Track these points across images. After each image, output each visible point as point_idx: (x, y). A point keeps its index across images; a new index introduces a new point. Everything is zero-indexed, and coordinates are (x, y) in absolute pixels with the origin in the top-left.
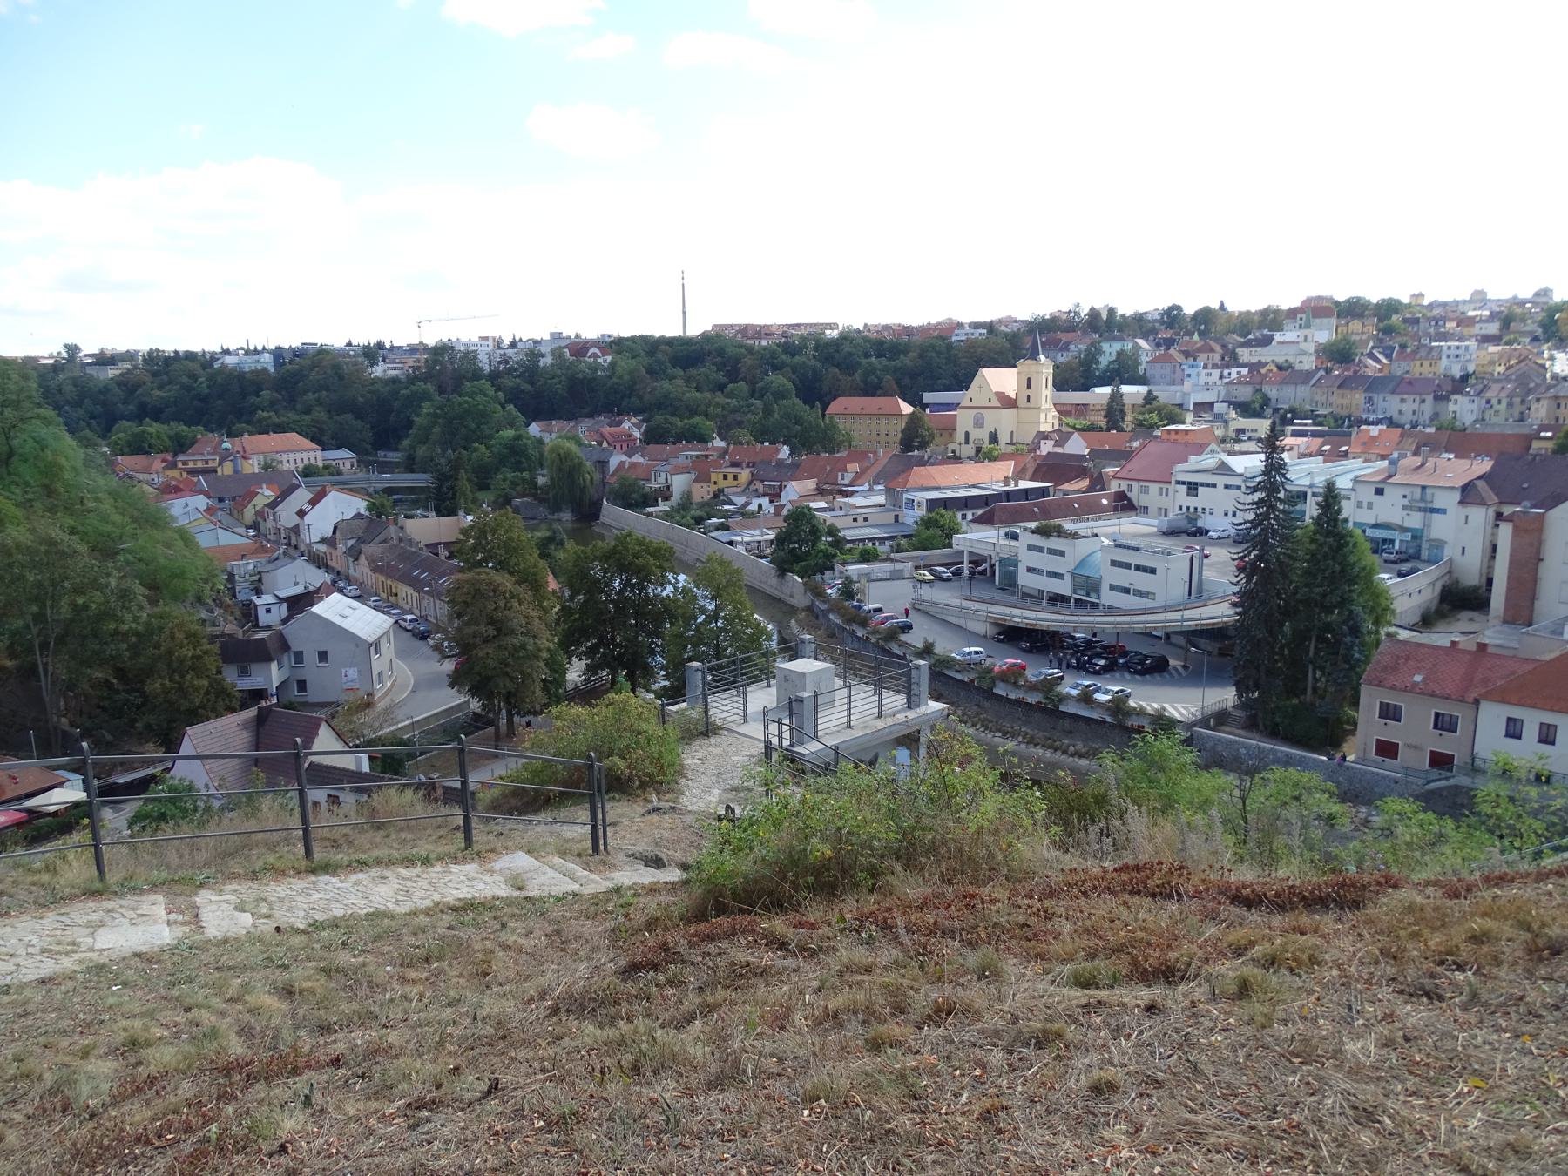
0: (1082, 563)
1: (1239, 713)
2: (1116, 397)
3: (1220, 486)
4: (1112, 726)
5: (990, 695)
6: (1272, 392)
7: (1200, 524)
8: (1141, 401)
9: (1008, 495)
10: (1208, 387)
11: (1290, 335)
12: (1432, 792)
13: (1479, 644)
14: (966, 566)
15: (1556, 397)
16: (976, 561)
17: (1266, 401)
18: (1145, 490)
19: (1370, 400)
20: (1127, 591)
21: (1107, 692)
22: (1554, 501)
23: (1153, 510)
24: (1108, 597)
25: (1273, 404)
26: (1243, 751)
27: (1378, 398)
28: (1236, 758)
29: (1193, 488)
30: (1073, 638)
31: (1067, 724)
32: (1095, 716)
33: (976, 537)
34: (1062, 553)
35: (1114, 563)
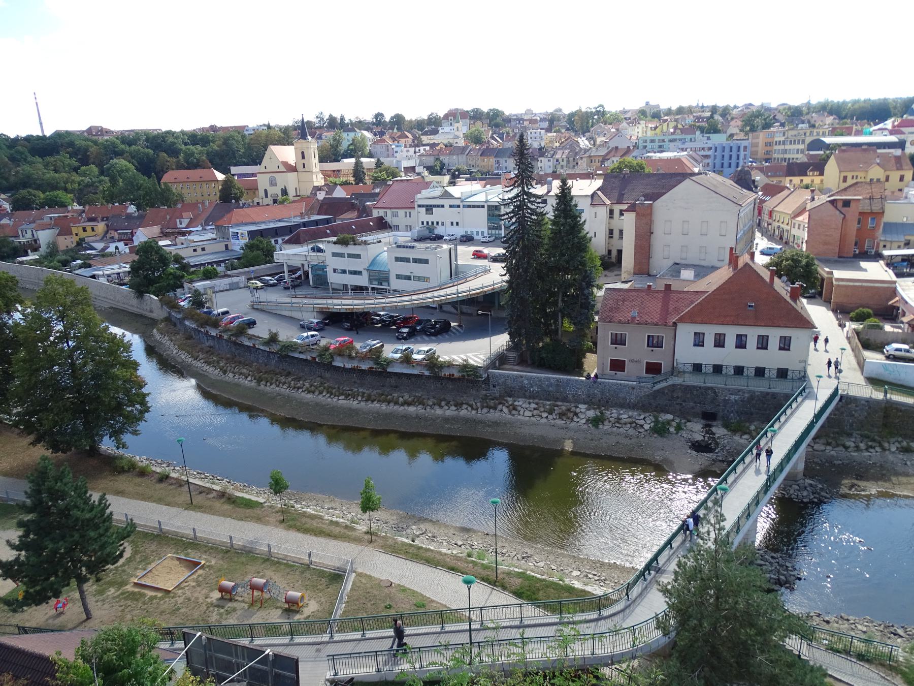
0: (373, 262)
1: (513, 354)
2: (358, 165)
3: (447, 206)
4: (428, 377)
5: (330, 367)
6: (445, 159)
7: (436, 232)
8: (374, 166)
9: (305, 224)
10: (408, 158)
11: (445, 129)
12: (658, 391)
13: (666, 285)
14: (286, 274)
15: (590, 156)
16: (293, 270)
17: (442, 165)
18: (396, 215)
19: (498, 162)
20: (409, 278)
21: (419, 352)
22: (655, 197)
23: (402, 227)
24: (395, 284)
26: (526, 382)
27: (502, 161)
28: (522, 388)
29: (429, 209)
30: (379, 315)
31: (393, 381)
33: (290, 254)
34: (358, 256)
35: (398, 259)
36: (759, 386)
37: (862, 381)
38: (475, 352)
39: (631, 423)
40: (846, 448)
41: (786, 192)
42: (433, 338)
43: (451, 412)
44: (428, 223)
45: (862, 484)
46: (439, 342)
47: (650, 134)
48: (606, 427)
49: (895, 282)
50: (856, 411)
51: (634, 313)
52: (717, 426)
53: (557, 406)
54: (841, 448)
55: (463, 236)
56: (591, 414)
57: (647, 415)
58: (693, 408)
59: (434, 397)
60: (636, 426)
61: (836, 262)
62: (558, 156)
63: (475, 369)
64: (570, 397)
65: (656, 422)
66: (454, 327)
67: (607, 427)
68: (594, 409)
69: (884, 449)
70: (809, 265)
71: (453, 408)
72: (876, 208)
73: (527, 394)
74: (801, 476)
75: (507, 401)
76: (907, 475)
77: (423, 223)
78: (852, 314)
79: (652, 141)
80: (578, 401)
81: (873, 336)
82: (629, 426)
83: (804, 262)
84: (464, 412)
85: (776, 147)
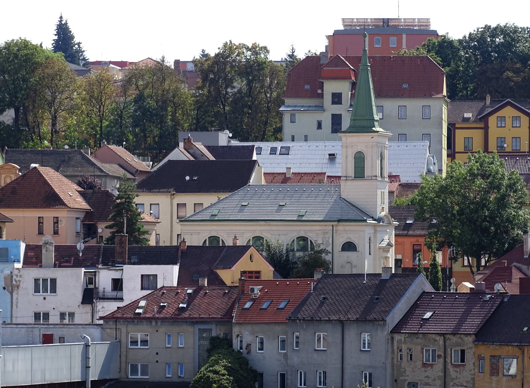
11: (299, 151)
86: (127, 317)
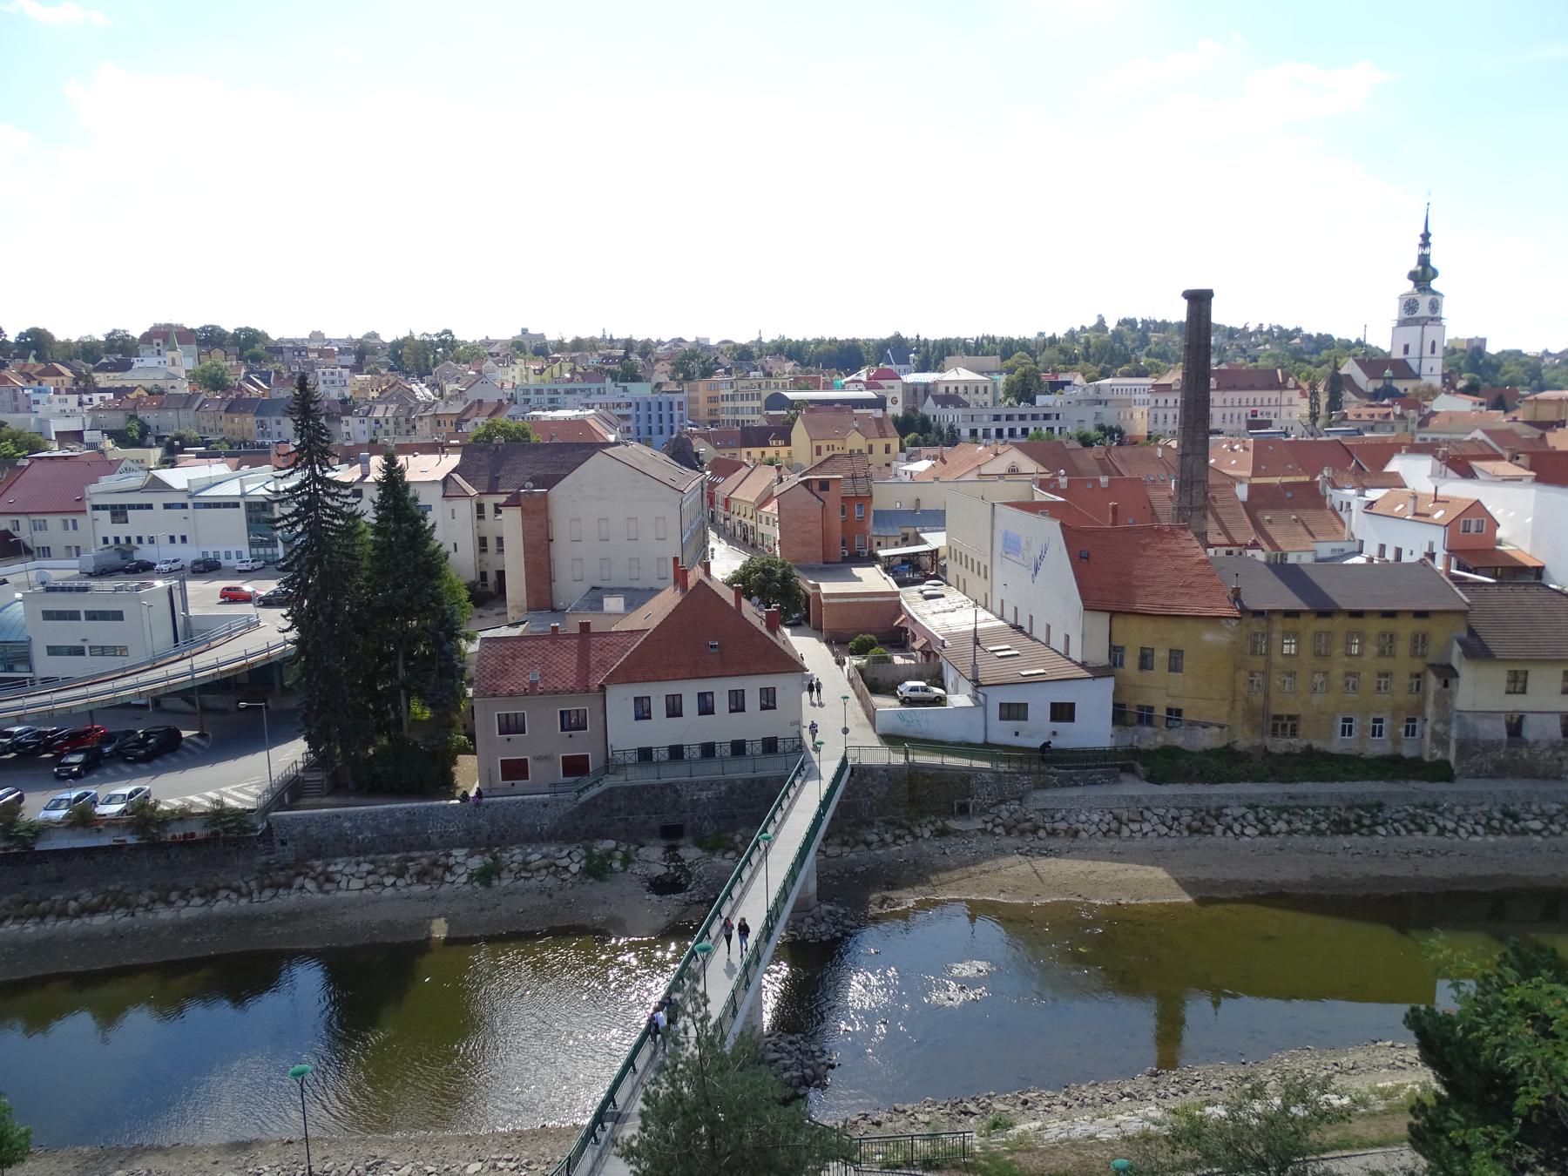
1: (318, 776)
3: (158, 506)
6: (151, 418)
7: (137, 556)
10: (64, 414)
12: (587, 803)
13: (581, 624)
15: (435, 415)
17: (145, 429)
18: (43, 527)
19: (262, 424)
20: (79, 651)
21: (110, 800)
22: (550, 481)
24: (44, 665)
25: (154, 429)
26: (347, 824)
27: (270, 421)
29: (119, 513)
30: (10, 735)
32: (106, 841)
35: (49, 615)
36: (740, 771)
37: (876, 742)
38: (239, 782)
39: (547, 867)
40: (868, 844)
41: (744, 471)
42: (143, 766)
43: (192, 910)
44: (117, 540)
45: (895, 894)
46: (157, 772)
47: (533, 380)
48: (505, 883)
49: (897, 594)
50: (873, 787)
51: (535, 675)
52: (685, 846)
53: (412, 860)
54: (862, 847)
55: (196, 562)
56: (476, 863)
57: (573, 847)
58: (646, 822)
59: (152, 887)
60: (556, 870)
61: (821, 569)
62: (378, 414)
63: (240, 816)
64: (435, 838)
65: (590, 857)
66: (188, 739)
67: (506, 881)
68: (481, 853)
69: (916, 838)
70: (786, 577)
71: (198, 901)
72: (861, 492)
73: (352, 847)
74: (814, 901)
75: (312, 868)
76: (948, 869)
77: (106, 540)
78: (851, 645)
79: (538, 392)
80: (449, 845)
81: (881, 673)
82: (544, 872)
83: (779, 572)
84: (221, 906)
85: (724, 404)
86: (97, 409)
